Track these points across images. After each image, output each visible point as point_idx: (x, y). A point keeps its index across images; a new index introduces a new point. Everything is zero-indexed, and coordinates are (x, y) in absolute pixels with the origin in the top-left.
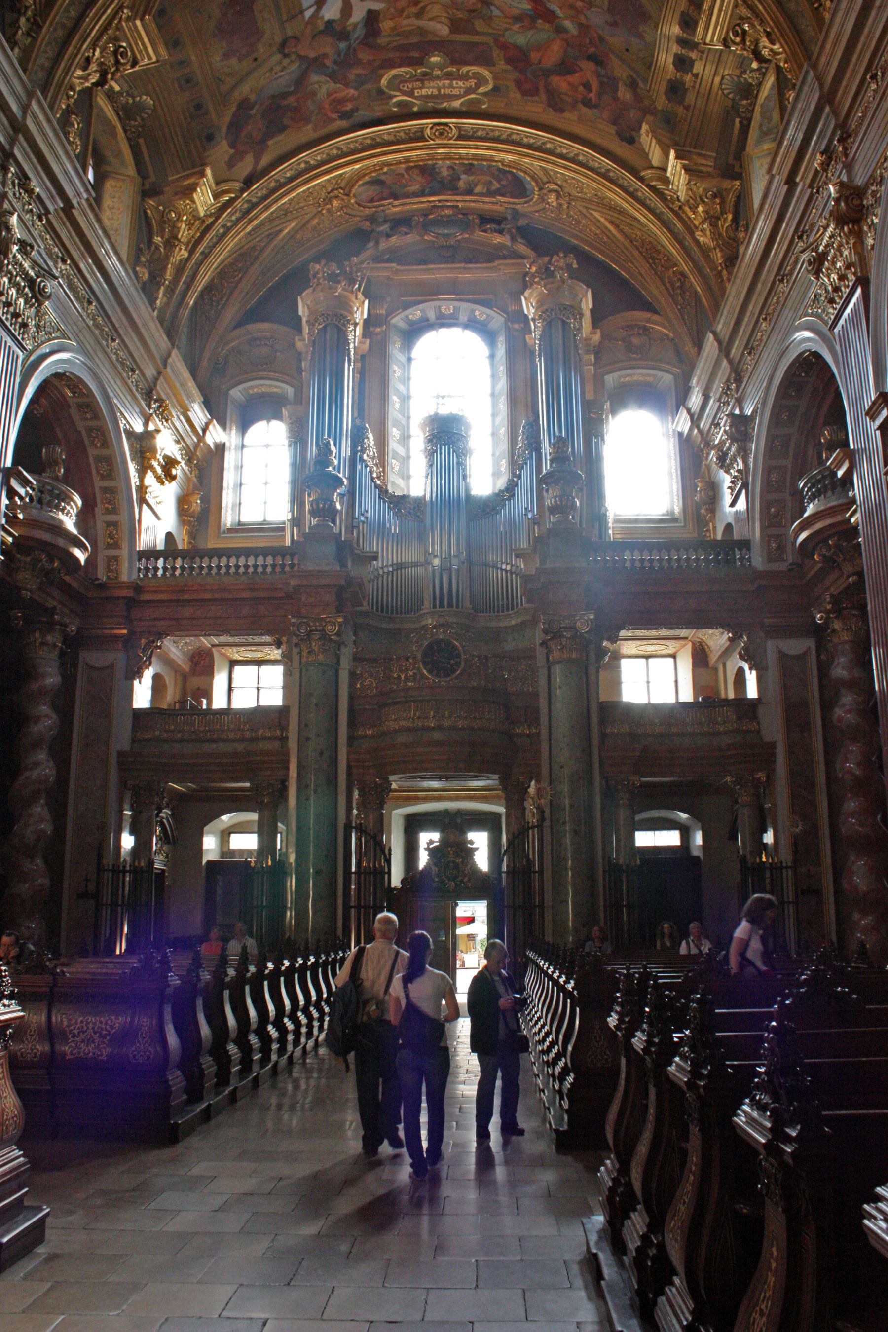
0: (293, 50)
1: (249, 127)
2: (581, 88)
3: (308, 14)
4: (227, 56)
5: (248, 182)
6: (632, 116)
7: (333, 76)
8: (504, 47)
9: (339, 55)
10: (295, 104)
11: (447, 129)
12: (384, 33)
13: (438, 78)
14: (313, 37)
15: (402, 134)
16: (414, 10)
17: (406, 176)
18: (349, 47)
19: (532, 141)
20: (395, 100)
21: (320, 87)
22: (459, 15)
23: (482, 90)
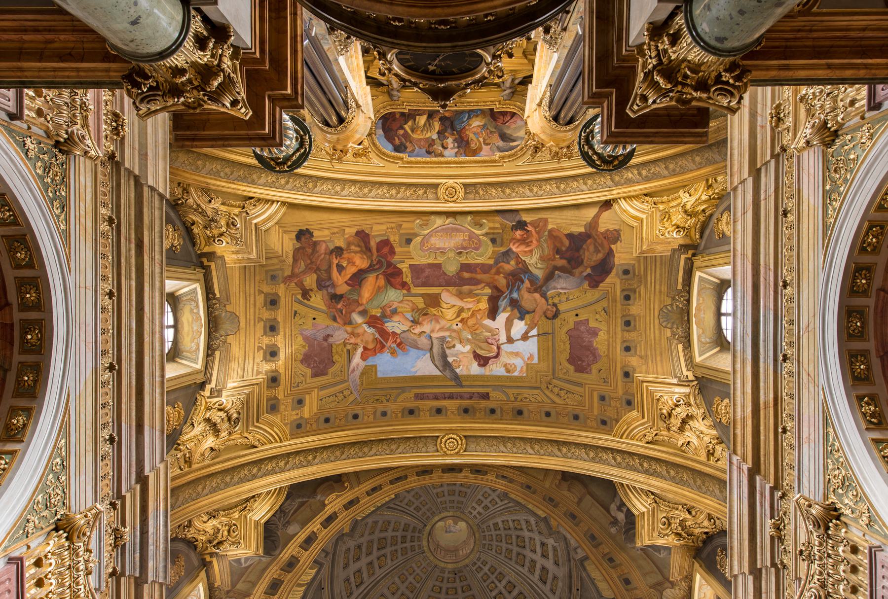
0: (549, 307)
1: (594, 259)
2: (345, 264)
3: (534, 332)
4: (594, 333)
5: (607, 204)
6: (302, 263)
7: (525, 269)
8: (404, 285)
9: (519, 287)
10: (557, 256)
11: (446, 197)
12: (486, 298)
13: (451, 250)
14: (534, 311)
15: (481, 192)
16: (464, 315)
17: (481, 140)
18: (511, 293)
19: (380, 191)
20: (484, 231)
21: (536, 264)
22: (433, 311)
23: (418, 239)
